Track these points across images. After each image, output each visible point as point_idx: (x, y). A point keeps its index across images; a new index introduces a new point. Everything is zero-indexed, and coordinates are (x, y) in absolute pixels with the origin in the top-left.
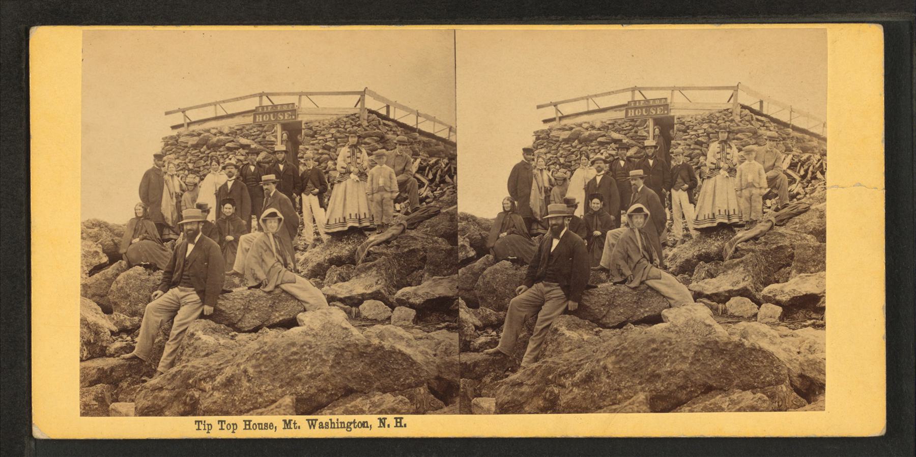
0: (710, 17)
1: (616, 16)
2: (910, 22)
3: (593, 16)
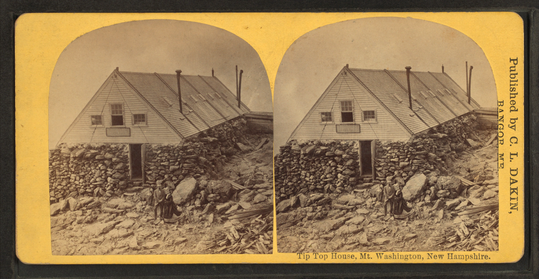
0: (411, 9)
1: (356, 8)
2: (527, 13)
3: (343, 8)
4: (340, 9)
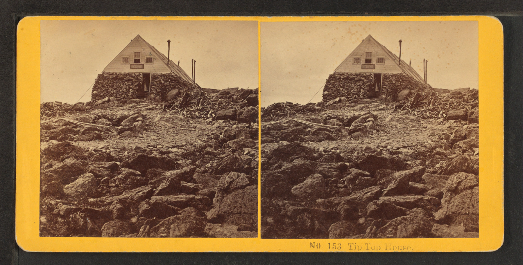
0: (408, 13)
3: (341, 12)
4: (339, 13)
